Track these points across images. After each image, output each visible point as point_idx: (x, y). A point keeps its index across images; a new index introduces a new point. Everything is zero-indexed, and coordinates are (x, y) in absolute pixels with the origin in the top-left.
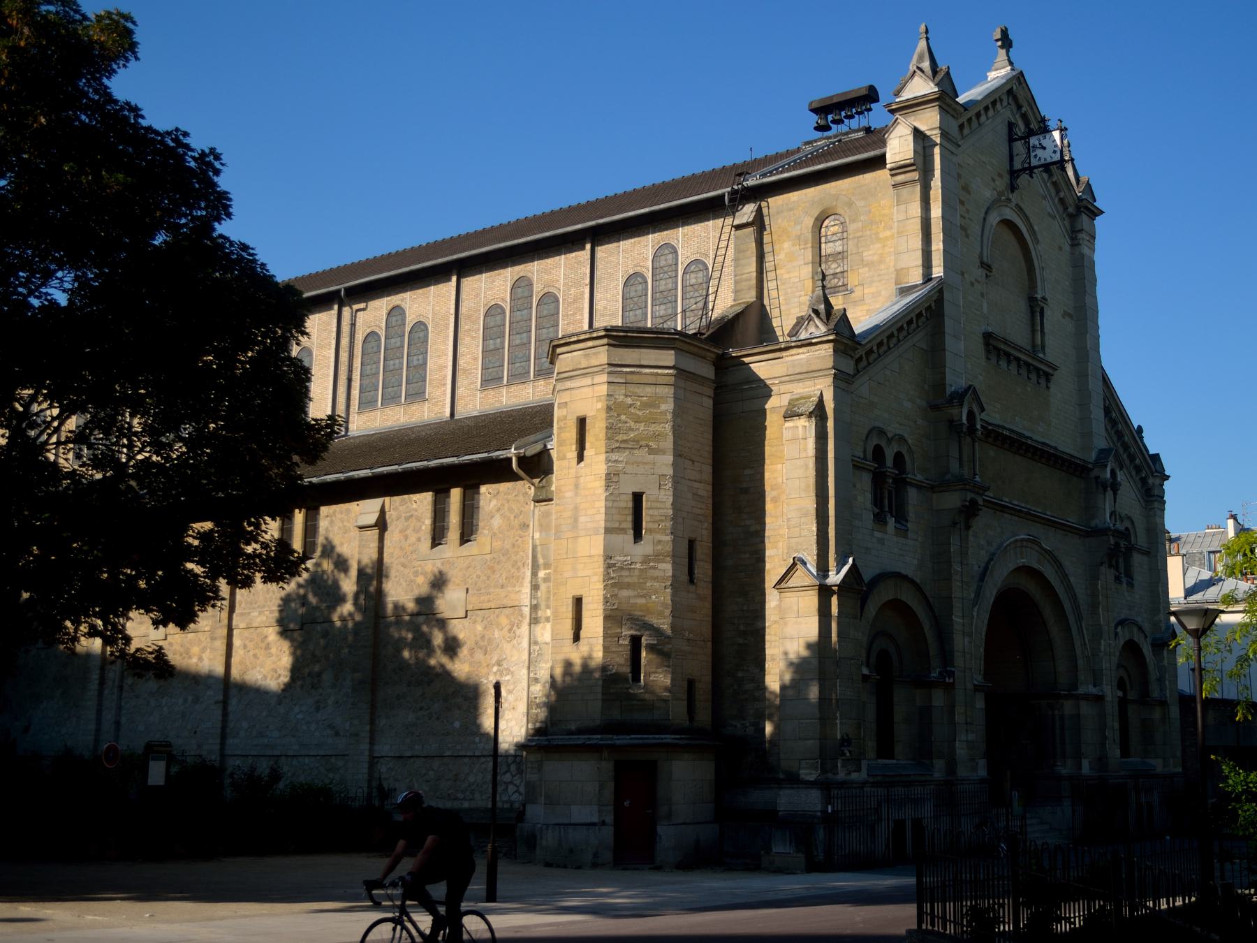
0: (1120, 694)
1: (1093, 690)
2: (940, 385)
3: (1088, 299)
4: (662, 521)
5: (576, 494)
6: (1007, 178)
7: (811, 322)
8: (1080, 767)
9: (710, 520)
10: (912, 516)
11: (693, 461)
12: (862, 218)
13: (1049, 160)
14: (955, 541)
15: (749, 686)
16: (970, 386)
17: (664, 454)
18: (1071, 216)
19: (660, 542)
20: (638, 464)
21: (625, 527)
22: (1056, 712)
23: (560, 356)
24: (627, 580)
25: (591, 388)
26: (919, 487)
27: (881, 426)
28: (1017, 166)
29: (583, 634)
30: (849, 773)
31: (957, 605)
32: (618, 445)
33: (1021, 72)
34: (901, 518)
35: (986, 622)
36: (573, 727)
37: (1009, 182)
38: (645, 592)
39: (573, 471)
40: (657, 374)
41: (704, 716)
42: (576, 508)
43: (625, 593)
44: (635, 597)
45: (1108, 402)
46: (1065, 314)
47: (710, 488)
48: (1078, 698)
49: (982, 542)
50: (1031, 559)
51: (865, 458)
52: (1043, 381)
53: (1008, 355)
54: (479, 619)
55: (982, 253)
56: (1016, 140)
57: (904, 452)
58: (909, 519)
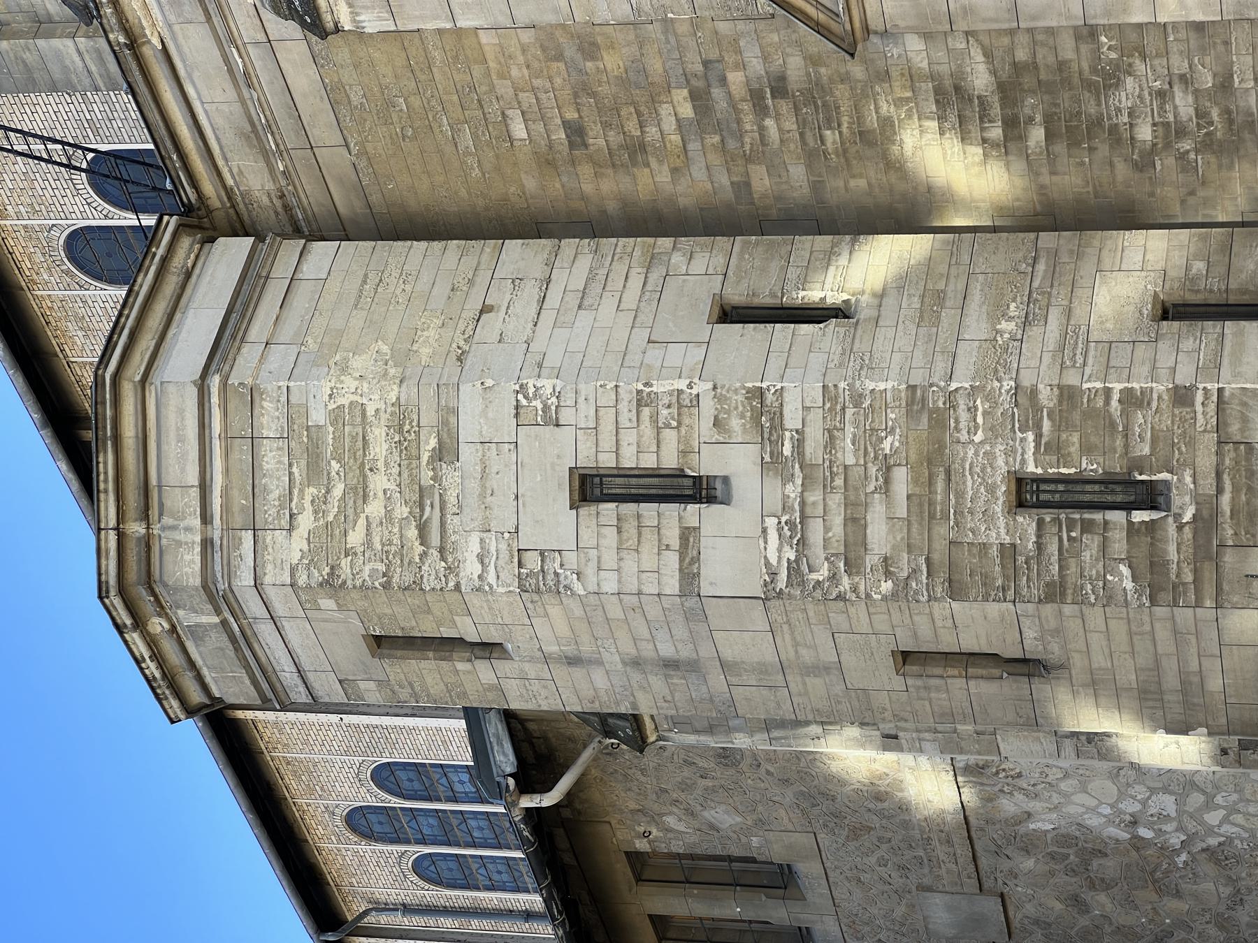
5: (600, 663)
9: (665, 243)
11: (485, 309)
15: (1184, 104)
21: (677, 532)
24: (837, 521)
25: (287, 625)
32: (435, 553)
38: (873, 470)
39: (531, 670)
40: (227, 438)
42: (636, 663)
43: (879, 536)
47: (569, 245)
54: (1005, 865)
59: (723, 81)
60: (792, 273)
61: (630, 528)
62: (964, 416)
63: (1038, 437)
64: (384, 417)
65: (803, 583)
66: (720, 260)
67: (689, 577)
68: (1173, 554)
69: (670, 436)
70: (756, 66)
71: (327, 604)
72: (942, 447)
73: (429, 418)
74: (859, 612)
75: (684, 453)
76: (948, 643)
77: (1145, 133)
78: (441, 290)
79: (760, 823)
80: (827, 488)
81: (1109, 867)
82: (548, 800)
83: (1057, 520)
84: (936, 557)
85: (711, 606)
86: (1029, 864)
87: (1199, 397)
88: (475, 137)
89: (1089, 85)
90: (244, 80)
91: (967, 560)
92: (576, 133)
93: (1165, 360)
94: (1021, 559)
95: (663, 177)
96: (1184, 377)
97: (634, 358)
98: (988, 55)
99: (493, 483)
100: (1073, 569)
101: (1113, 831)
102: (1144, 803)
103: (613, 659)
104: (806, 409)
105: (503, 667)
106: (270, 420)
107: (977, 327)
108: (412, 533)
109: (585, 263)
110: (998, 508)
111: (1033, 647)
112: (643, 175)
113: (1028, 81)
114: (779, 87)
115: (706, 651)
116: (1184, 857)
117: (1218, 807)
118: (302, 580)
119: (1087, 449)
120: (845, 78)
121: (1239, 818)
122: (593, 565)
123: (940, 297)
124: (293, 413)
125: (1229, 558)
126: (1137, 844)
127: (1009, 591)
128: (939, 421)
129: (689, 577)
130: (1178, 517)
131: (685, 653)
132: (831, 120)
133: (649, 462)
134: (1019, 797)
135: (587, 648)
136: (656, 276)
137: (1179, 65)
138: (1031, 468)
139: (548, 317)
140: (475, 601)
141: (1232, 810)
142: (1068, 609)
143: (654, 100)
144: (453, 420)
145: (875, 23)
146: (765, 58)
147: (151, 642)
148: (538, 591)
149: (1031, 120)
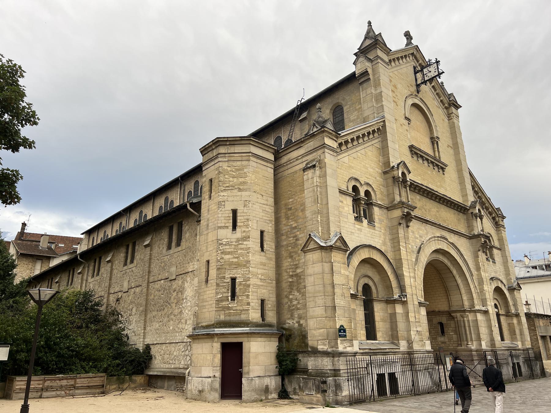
0: (496, 310)
1: (484, 309)
2: (387, 163)
3: (459, 140)
4: (245, 222)
5: (208, 214)
6: (415, 88)
7: (315, 126)
8: (481, 345)
12: (349, 103)
13: (433, 76)
14: (401, 232)
15: (295, 303)
16: (402, 162)
18: (446, 108)
20: (234, 196)
22: (465, 319)
24: (229, 250)
25: (214, 166)
26: (380, 206)
27: (356, 177)
28: (419, 82)
31: (405, 263)
32: (224, 188)
33: (417, 46)
34: (371, 222)
35: (423, 273)
37: (416, 89)
38: (237, 256)
39: (207, 204)
40: (242, 156)
43: (227, 257)
45: (473, 184)
46: (448, 146)
47: (273, 208)
49: (417, 236)
50: (444, 246)
51: (348, 190)
52: (440, 170)
54: (180, 279)
55: (405, 114)
56: (418, 72)
58: (375, 221)
59: (298, 231)
60: (269, 242)
61: (228, 218)
62: (245, 270)
63: (242, 282)
64: (245, 180)
65: (219, 245)
66: (270, 231)
67: (220, 228)
68: (223, 303)
69: (242, 224)
71: (217, 172)
72: (240, 266)
73: (245, 187)
74: (215, 254)
75: (240, 226)
76: (210, 268)
77: (291, 297)
78: (265, 189)
79: (187, 241)
80: (234, 249)
81: (180, 295)
82: (188, 207)
83: (229, 285)
84: (224, 266)
85: (216, 231)
86: (180, 283)
87: (248, 307)
88: (289, 194)
89: (297, 288)
90: (297, 159)
91: (223, 271)
93: (254, 301)
94: (223, 279)
95: (284, 223)
96: (252, 304)
97: (254, 218)
98: (302, 272)
99: (235, 197)
100: (221, 288)
101: (185, 296)
102: (189, 300)
103: (209, 216)
104: (246, 245)
105: (208, 200)
106: (244, 163)
107: (260, 271)
108: (227, 185)
109: (270, 211)
110: (231, 276)
111: (209, 282)
112: (284, 219)
113: (298, 278)
115: (210, 231)
116: (181, 307)
117: (188, 312)
118: (220, 168)
119: (240, 289)
120: (298, 250)
121: (187, 315)
122: (223, 213)
124: (246, 166)
125: (223, 312)
126: (183, 299)
127: (218, 277)
128: (245, 266)
129: (220, 228)
130: (229, 304)
131: (209, 228)
132: (293, 248)
133: (238, 221)
134: (190, 281)
135: (210, 212)
136: (268, 221)
137: (301, 302)
138: (237, 281)
139: (261, 205)
140: (217, 195)
141: (188, 314)
142: (215, 287)
143: (295, 220)
144: (245, 191)
145: (305, 254)
146: (301, 237)
147: (211, 146)
148: (219, 204)
149: (293, 279)
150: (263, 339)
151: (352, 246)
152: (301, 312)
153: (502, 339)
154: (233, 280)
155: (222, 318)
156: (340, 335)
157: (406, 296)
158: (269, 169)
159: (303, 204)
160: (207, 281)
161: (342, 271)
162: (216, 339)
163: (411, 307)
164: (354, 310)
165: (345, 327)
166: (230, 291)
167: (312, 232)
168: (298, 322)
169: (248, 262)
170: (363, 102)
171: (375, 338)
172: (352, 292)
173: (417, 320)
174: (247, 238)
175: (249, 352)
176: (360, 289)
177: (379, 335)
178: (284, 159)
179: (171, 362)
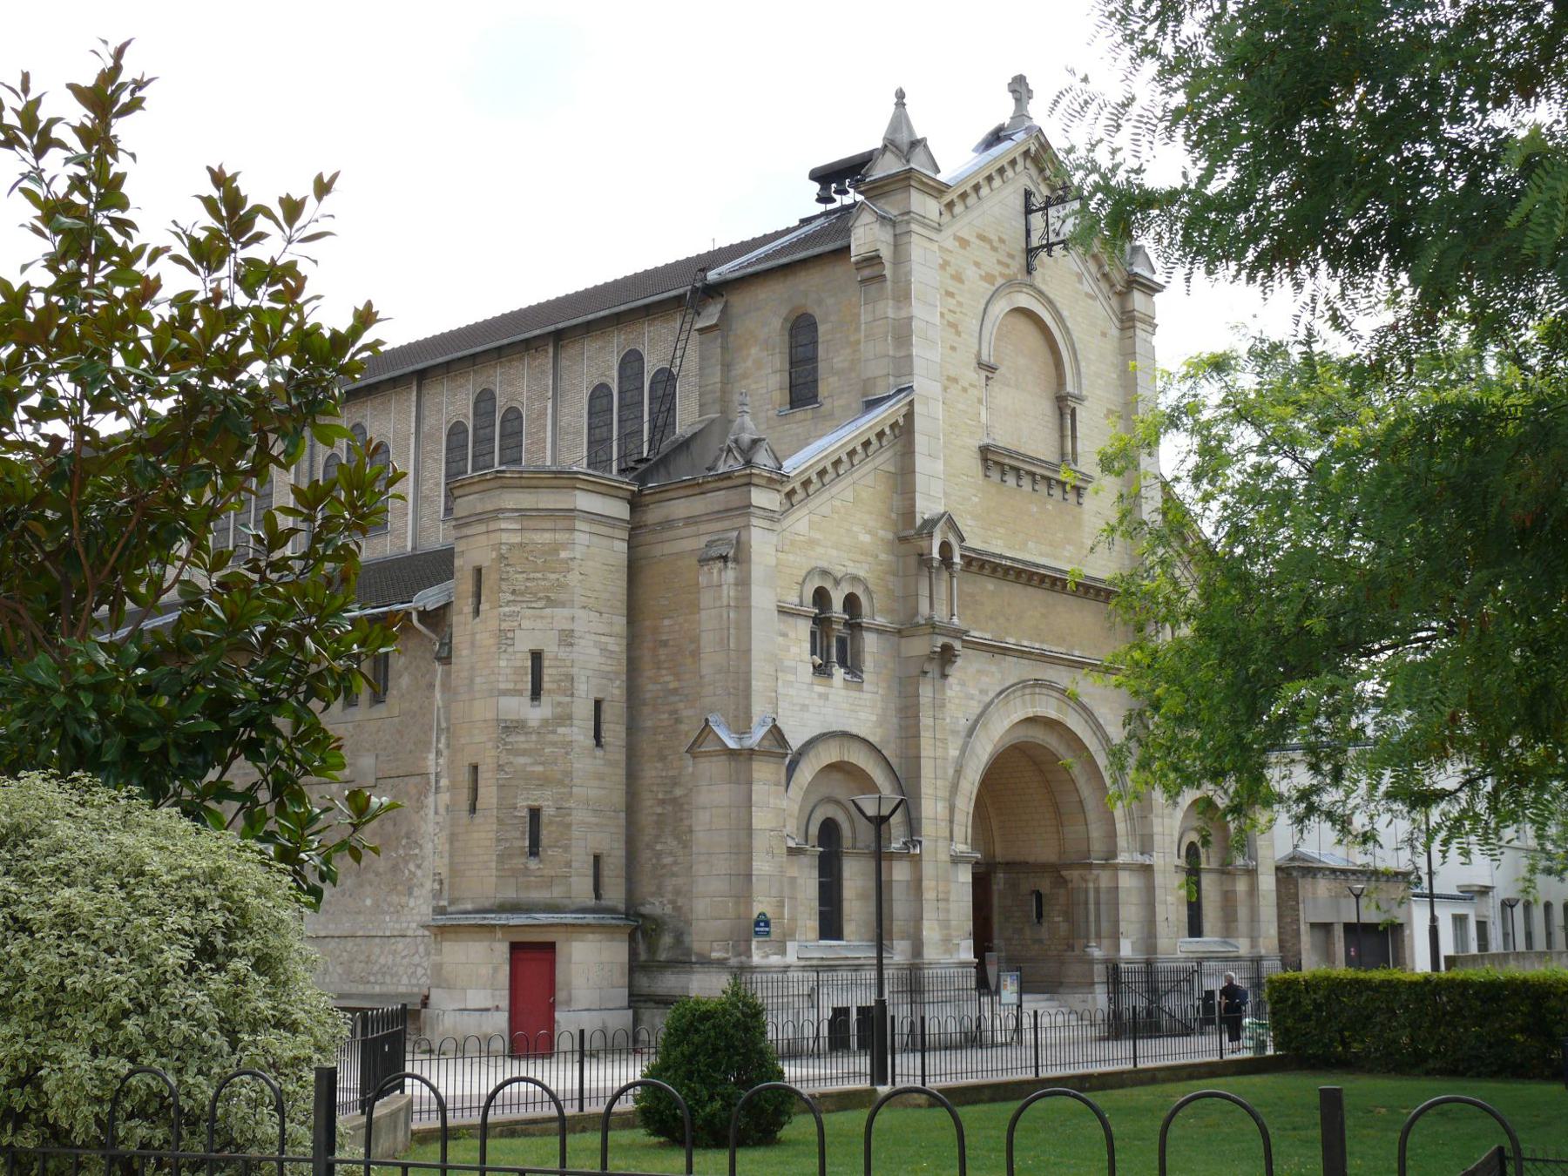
1: (1139, 859)
2: (909, 513)
8: (1117, 948)
9: (624, 677)
10: (869, 664)
11: (601, 613)
14: (926, 692)
15: (667, 860)
17: (564, 607)
18: (1120, 294)
19: (559, 704)
22: (1091, 885)
23: (458, 500)
28: (1035, 242)
29: (478, 806)
30: (767, 956)
34: (853, 668)
36: (469, 907)
37: (1024, 263)
41: (615, 895)
42: (472, 668)
43: (522, 760)
44: (532, 764)
46: (1110, 412)
47: (624, 642)
48: (1116, 868)
49: (975, 692)
50: (1049, 708)
52: (1071, 497)
53: (1017, 470)
55: (979, 354)
57: (859, 592)
70: (685, 713)
71: (494, 555)
75: (549, 691)
76: (481, 783)
77: (658, 847)
92: (665, 644)
98: (686, 795)
110: (530, 803)
114: (678, 721)
123: (602, 779)
124: (564, 546)
125: (513, 880)
128: (560, 783)
129: (504, 693)
133: (546, 678)
139: (597, 638)
142: (495, 827)
150: (597, 936)
151: (795, 742)
152: (680, 881)
153: (1195, 929)
154: (535, 813)
155: (510, 894)
156: (756, 933)
157: (920, 842)
158: (617, 543)
159: (696, 640)
160: (473, 809)
161: (772, 801)
162: (499, 935)
163: (928, 869)
164: (793, 880)
165: (768, 915)
166: (527, 836)
167: (711, 711)
168: (673, 902)
169: (568, 774)
170: (866, 336)
171: (838, 935)
172: (792, 844)
173: (941, 896)
174: (565, 719)
175: (570, 961)
176: (814, 830)
177: (849, 928)
178: (654, 515)
179: (372, 979)
